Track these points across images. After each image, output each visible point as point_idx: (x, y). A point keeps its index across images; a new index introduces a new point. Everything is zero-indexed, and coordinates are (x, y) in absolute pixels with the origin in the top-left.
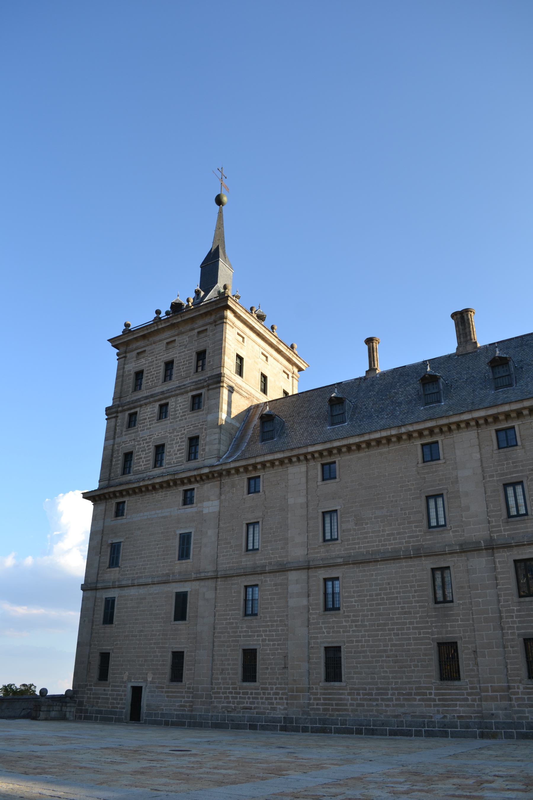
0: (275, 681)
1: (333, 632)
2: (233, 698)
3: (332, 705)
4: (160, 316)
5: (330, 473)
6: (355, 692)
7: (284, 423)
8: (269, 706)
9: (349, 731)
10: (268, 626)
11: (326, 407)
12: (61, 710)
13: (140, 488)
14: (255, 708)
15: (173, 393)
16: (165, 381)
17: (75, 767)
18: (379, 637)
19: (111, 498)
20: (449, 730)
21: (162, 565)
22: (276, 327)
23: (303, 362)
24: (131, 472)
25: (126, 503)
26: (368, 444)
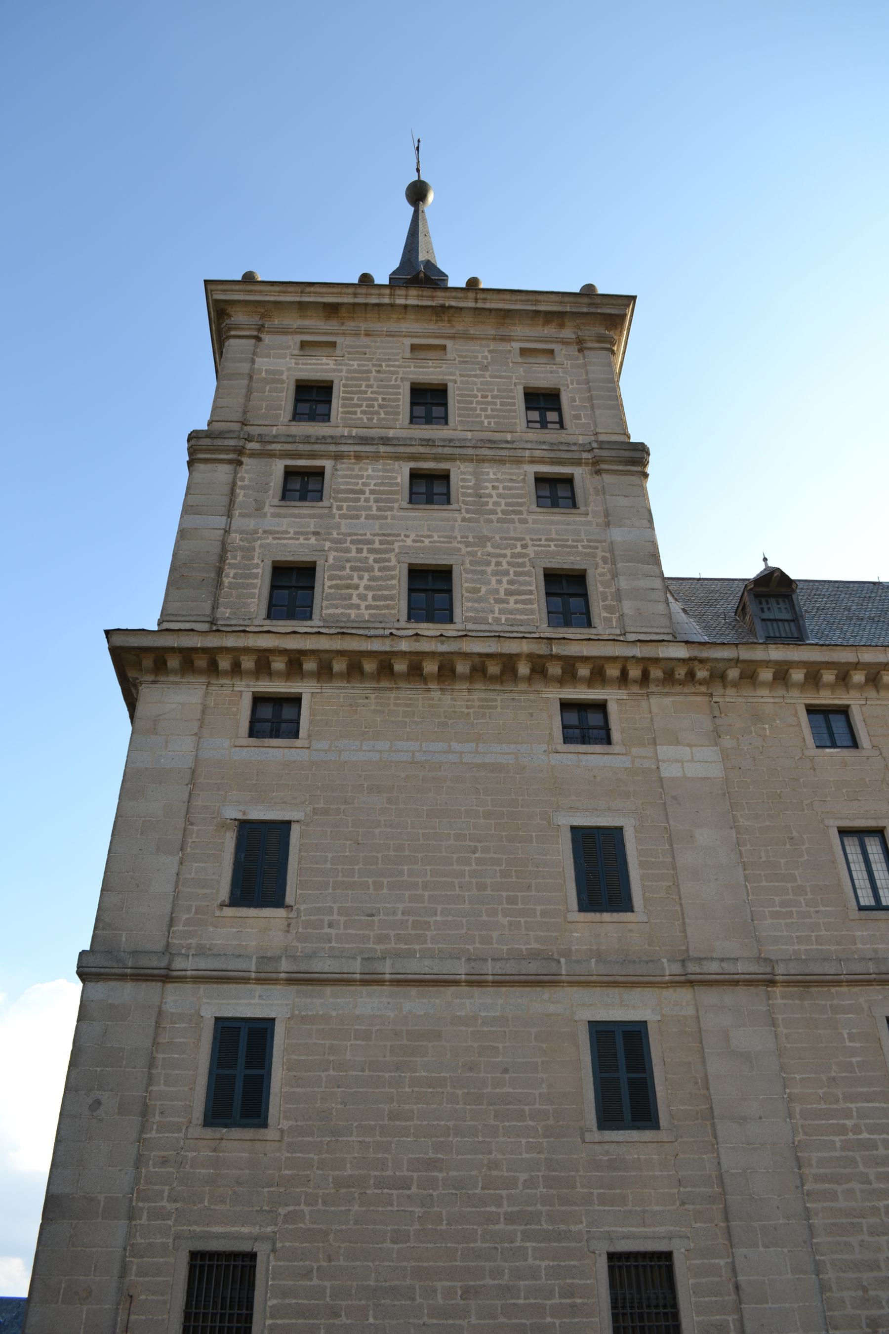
21: (505, 921)
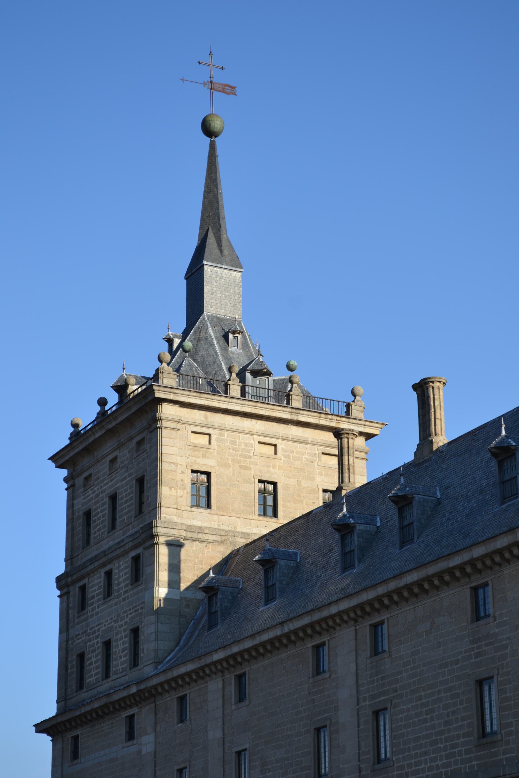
15: (114, 554)
23: (367, 423)
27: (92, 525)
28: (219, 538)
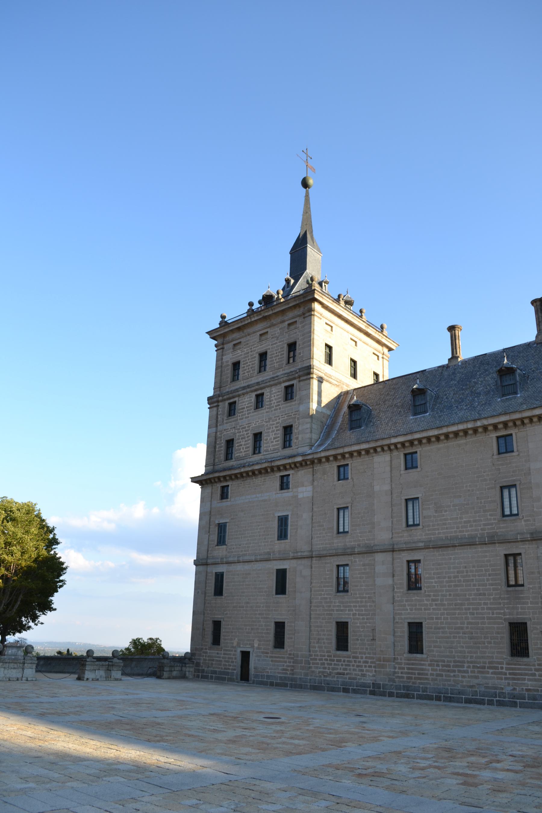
0: (365, 651)
1: (415, 609)
2: (328, 664)
3: (415, 674)
4: (254, 308)
5: (412, 462)
6: (435, 663)
7: (371, 411)
8: (360, 673)
9: (430, 698)
10: (358, 602)
11: (410, 397)
12: (182, 670)
13: (241, 474)
14: (347, 674)
16: (260, 371)
17: (186, 735)
18: (457, 616)
19: (216, 482)
20: (518, 701)
21: (263, 544)
22: (364, 311)
23: (392, 343)
24: (233, 458)
25: (230, 488)
26: (447, 436)
27: (241, 370)
28: (336, 383)
